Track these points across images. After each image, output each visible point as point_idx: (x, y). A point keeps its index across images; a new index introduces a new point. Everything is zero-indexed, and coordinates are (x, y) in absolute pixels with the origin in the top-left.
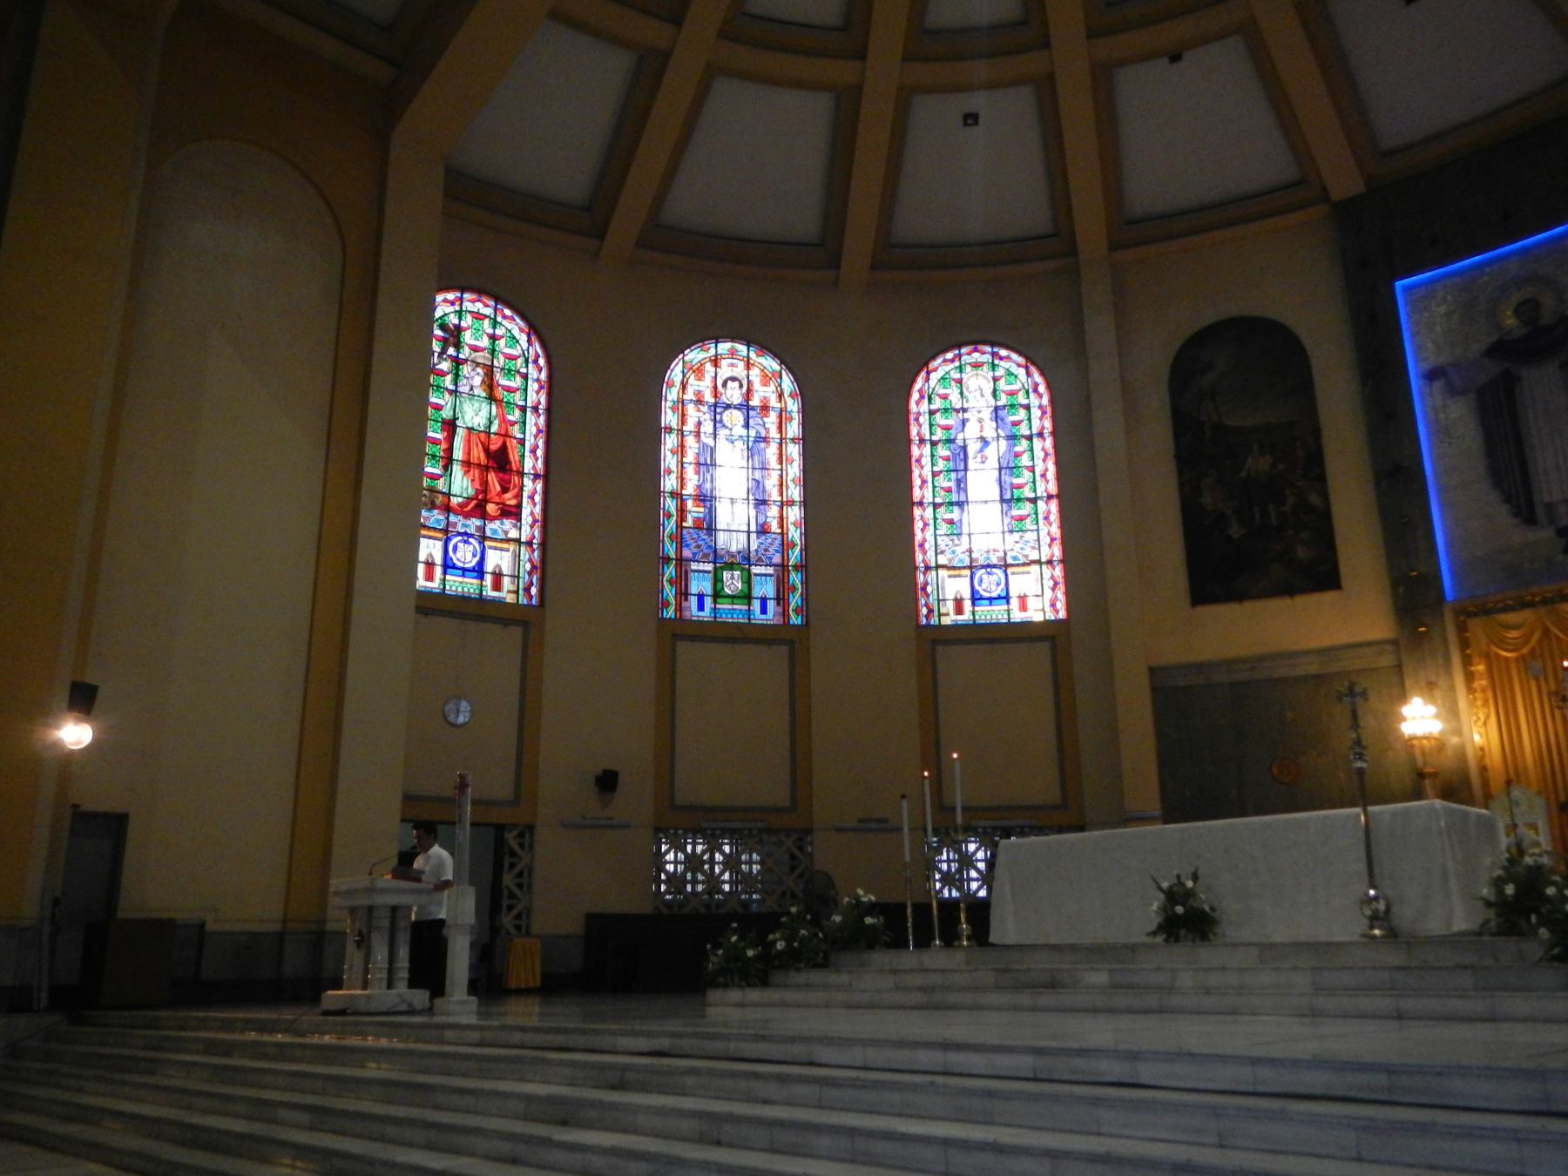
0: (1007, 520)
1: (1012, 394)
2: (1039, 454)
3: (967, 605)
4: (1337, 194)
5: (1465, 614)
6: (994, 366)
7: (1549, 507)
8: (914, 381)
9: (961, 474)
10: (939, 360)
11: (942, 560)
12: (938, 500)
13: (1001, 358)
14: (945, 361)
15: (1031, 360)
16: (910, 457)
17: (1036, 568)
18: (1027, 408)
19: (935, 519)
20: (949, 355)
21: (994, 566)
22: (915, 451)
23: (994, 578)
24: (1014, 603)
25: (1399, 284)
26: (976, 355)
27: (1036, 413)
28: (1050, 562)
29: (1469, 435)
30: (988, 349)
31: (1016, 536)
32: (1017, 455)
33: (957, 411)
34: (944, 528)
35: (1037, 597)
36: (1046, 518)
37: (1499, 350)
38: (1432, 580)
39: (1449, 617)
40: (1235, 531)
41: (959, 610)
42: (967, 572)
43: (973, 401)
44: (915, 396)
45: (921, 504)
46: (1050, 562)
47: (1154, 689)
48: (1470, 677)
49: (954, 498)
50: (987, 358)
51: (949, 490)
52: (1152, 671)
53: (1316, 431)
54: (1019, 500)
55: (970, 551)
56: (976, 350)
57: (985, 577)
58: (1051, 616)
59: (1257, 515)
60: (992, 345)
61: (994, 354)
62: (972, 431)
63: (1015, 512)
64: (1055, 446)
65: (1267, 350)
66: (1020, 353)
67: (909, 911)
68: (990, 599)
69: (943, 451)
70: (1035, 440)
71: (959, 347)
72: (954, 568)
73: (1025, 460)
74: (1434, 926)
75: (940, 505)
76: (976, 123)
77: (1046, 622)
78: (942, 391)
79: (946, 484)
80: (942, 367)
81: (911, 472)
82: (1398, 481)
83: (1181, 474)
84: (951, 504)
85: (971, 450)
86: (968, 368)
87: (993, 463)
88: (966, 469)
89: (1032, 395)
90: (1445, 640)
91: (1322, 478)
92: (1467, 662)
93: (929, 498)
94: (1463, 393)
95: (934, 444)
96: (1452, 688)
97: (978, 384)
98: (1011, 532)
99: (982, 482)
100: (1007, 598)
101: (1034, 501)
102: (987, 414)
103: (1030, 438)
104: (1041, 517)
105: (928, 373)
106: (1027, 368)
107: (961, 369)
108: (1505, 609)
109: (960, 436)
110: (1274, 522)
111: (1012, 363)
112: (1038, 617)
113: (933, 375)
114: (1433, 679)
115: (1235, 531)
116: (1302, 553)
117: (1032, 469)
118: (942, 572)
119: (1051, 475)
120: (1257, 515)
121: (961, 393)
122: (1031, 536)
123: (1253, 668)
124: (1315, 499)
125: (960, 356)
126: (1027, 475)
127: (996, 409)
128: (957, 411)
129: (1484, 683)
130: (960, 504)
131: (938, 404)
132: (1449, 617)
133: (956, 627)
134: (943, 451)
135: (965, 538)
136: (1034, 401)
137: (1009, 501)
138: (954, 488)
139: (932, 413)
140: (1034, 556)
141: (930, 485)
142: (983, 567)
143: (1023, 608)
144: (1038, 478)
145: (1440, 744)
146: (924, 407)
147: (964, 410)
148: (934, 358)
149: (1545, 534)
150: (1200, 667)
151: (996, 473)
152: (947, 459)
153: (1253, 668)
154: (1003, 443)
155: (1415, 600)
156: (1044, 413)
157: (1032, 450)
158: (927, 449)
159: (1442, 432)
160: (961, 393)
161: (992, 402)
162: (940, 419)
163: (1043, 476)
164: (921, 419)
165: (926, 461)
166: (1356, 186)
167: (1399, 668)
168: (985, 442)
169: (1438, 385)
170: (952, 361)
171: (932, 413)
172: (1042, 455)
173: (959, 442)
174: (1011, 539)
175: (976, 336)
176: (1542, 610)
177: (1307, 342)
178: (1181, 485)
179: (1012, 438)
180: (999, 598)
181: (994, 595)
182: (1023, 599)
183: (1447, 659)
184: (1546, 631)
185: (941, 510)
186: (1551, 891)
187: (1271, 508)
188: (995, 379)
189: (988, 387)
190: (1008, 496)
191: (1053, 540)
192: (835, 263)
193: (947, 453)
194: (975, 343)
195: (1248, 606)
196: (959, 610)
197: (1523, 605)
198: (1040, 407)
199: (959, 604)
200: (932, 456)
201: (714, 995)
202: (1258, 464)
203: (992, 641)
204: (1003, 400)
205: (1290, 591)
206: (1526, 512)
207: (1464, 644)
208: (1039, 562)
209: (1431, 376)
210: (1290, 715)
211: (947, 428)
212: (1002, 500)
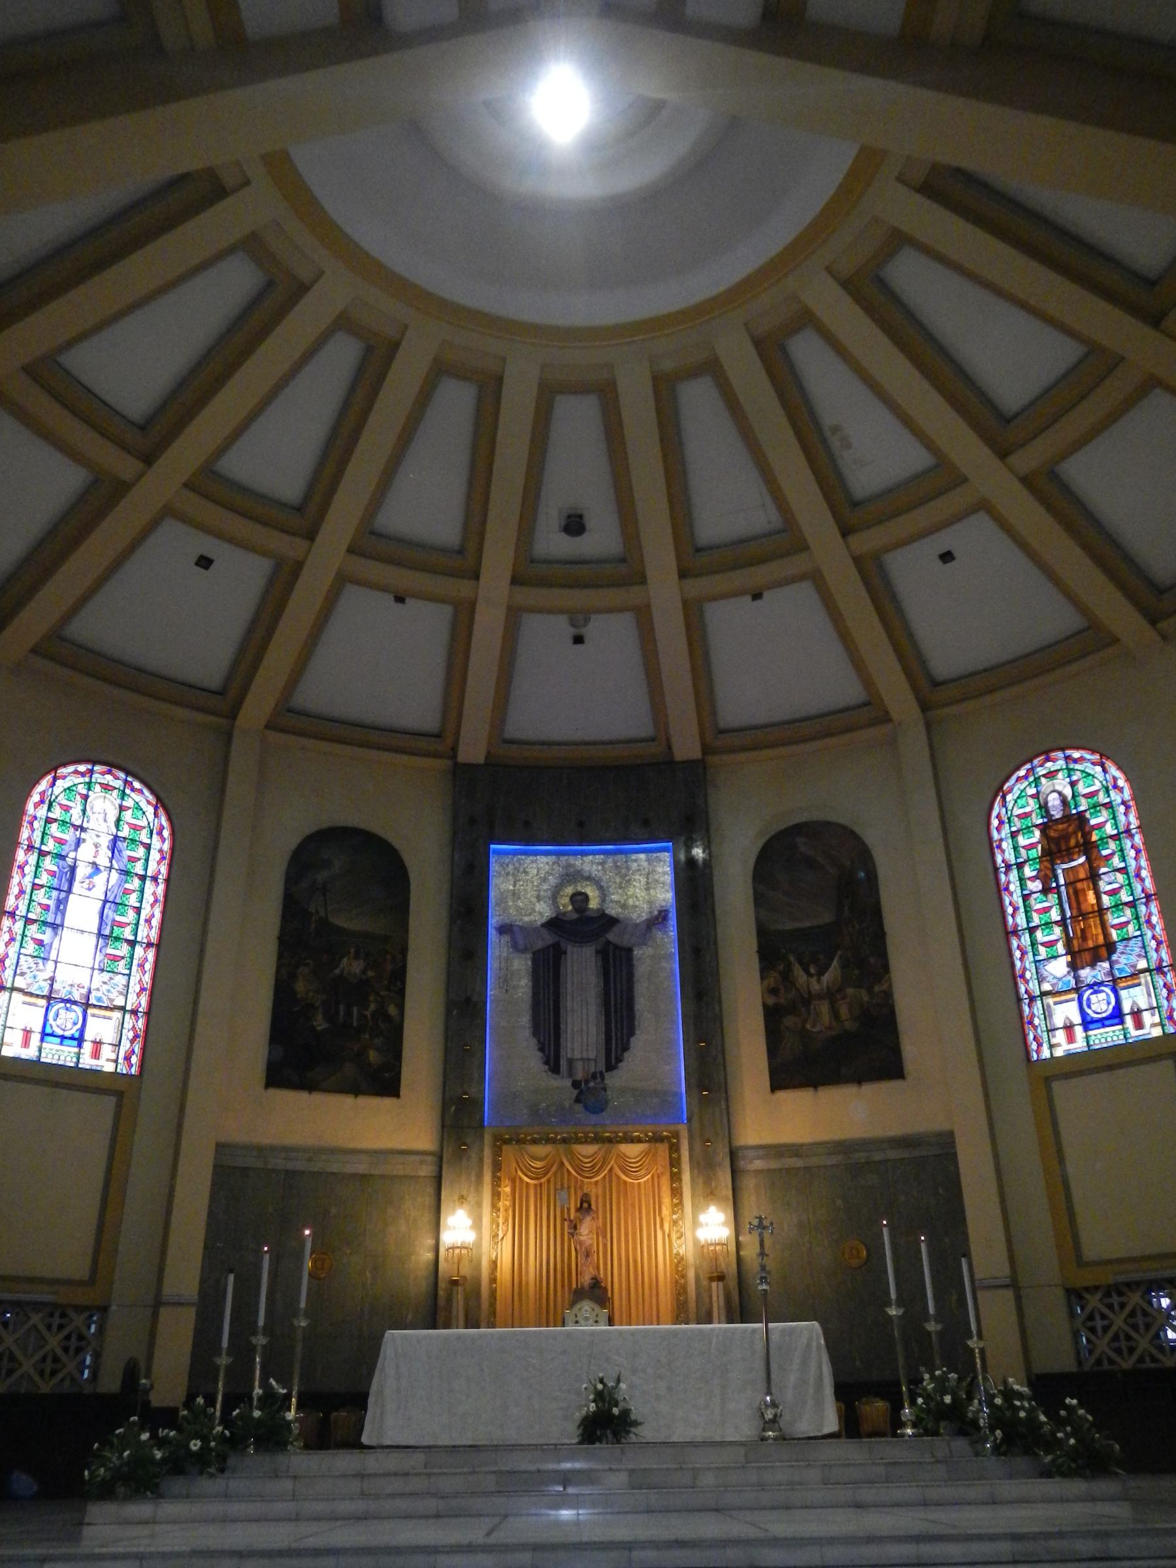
0: (99, 957)
1: (135, 828)
2: (148, 898)
3: (35, 1038)
4: (462, 758)
5: (500, 1141)
6: (123, 795)
7: (570, 1061)
8: (37, 782)
9: (63, 895)
10: (71, 769)
11: (20, 982)
12: (31, 916)
13: (133, 790)
14: (76, 772)
15: (161, 803)
16: (14, 860)
17: (117, 1015)
18: (148, 847)
19: (23, 935)
20: (82, 768)
21: (75, 1003)
22: (20, 856)
23: (73, 1015)
24: (87, 1047)
25: (492, 846)
26: (109, 777)
27: (155, 856)
28: (134, 1012)
29: (523, 986)
30: (122, 775)
31: (106, 976)
32: (127, 892)
33: (76, 827)
34: (30, 947)
35: (109, 1044)
36: (141, 966)
37: (555, 924)
38: (476, 1104)
39: (488, 1139)
40: (320, 1023)
41: (26, 1043)
42: (43, 1002)
43: (92, 823)
44: (35, 797)
45: (12, 915)
46: (134, 1012)
47: (215, 1166)
48: (496, 1195)
49: (50, 918)
50: (118, 784)
51: (46, 908)
52: (220, 1147)
53: (404, 950)
54: (117, 939)
55: (52, 979)
56: (109, 772)
57: (62, 1012)
58: (122, 1068)
59: (342, 1013)
60: (128, 773)
61: (126, 782)
62: (85, 853)
63: (110, 951)
64: (166, 896)
65: (374, 864)
66: (153, 792)
68: (63, 1038)
69: (49, 864)
70: (148, 882)
71: (94, 763)
72: (31, 994)
73: (133, 900)
74: (804, 1427)
75: (34, 921)
76: (207, 568)
77: (115, 1073)
78: (65, 802)
79: (46, 902)
80: (70, 777)
81: (10, 877)
82: (464, 1011)
83: (280, 957)
84: (45, 923)
85: (82, 871)
86: (98, 788)
87: (99, 892)
88: (69, 891)
89: (155, 836)
90: (481, 1160)
91: (401, 993)
92: (496, 1182)
93: (22, 910)
94: (525, 950)
95: (42, 854)
96: (479, 1205)
97: (103, 806)
98: (102, 970)
100: (80, 1040)
101: (132, 944)
102: (105, 841)
103: (143, 878)
104: (135, 962)
105: (55, 779)
106: (156, 808)
107: (89, 785)
108: (535, 1142)
109: (72, 855)
110: (355, 1024)
111: (143, 799)
112: (109, 1068)
113: (59, 782)
114: (465, 1193)
115: (320, 1023)
116: (373, 1056)
117: (138, 910)
118: (15, 994)
119: (155, 922)
120: (342, 1013)
121: (84, 811)
122: (121, 980)
123: (310, 1160)
124: (392, 1010)
125: (91, 772)
126: (131, 916)
127: (116, 838)
128: (76, 827)
129: (508, 1203)
130: (56, 927)
131: (57, 813)
132: (488, 1139)
133: (16, 1060)
134: (49, 864)
135: (50, 965)
136: (156, 843)
137: (106, 937)
138: (52, 908)
139: (49, 821)
140: (120, 1001)
141: (27, 896)
142: (63, 1001)
143: (96, 1054)
144: (142, 922)
146: (42, 812)
147: (83, 829)
148: (65, 765)
150: (261, 1150)
151: (100, 903)
152: (53, 874)
153: (310, 1160)
154: (115, 876)
155: (460, 1120)
156: (163, 858)
157: (142, 891)
158: (33, 858)
159: (506, 981)
160: (84, 811)
161: (114, 831)
162: (54, 829)
163: (148, 921)
164: (36, 824)
165: (27, 869)
166: (481, 759)
167: (438, 1181)
168: (96, 868)
169: (506, 938)
170: (83, 774)
171: (49, 821)
172: (152, 899)
173: (69, 861)
174: (99, 978)
175: (130, 767)
176: (561, 1147)
178: (279, 967)
179: (125, 873)
180: (72, 1038)
181: (68, 1034)
182: (98, 1044)
183: (480, 1176)
184: (562, 1164)
185: (33, 930)
186: (948, 1399)
187: (355, 1009)
188: (122, 808)
189: (113, 815)
190: (107, 932)
191: (143, 989)
193: (55, 868)
194: (112, 766)
195: (317, 1098)
196: (26, 1043)
197: (548, 1141)
198: (161, 851)
199: (27, 1033)
200: (38, 866)
201: (97, 1511)
202: (351, 966)
203: (56, 1085)
204: (125, 832)
205: (356, 1090)
207: (497, 1167)
208: (123, 1009)
210: (334, 1211)
211: (61, 842)
212: (100, 934)
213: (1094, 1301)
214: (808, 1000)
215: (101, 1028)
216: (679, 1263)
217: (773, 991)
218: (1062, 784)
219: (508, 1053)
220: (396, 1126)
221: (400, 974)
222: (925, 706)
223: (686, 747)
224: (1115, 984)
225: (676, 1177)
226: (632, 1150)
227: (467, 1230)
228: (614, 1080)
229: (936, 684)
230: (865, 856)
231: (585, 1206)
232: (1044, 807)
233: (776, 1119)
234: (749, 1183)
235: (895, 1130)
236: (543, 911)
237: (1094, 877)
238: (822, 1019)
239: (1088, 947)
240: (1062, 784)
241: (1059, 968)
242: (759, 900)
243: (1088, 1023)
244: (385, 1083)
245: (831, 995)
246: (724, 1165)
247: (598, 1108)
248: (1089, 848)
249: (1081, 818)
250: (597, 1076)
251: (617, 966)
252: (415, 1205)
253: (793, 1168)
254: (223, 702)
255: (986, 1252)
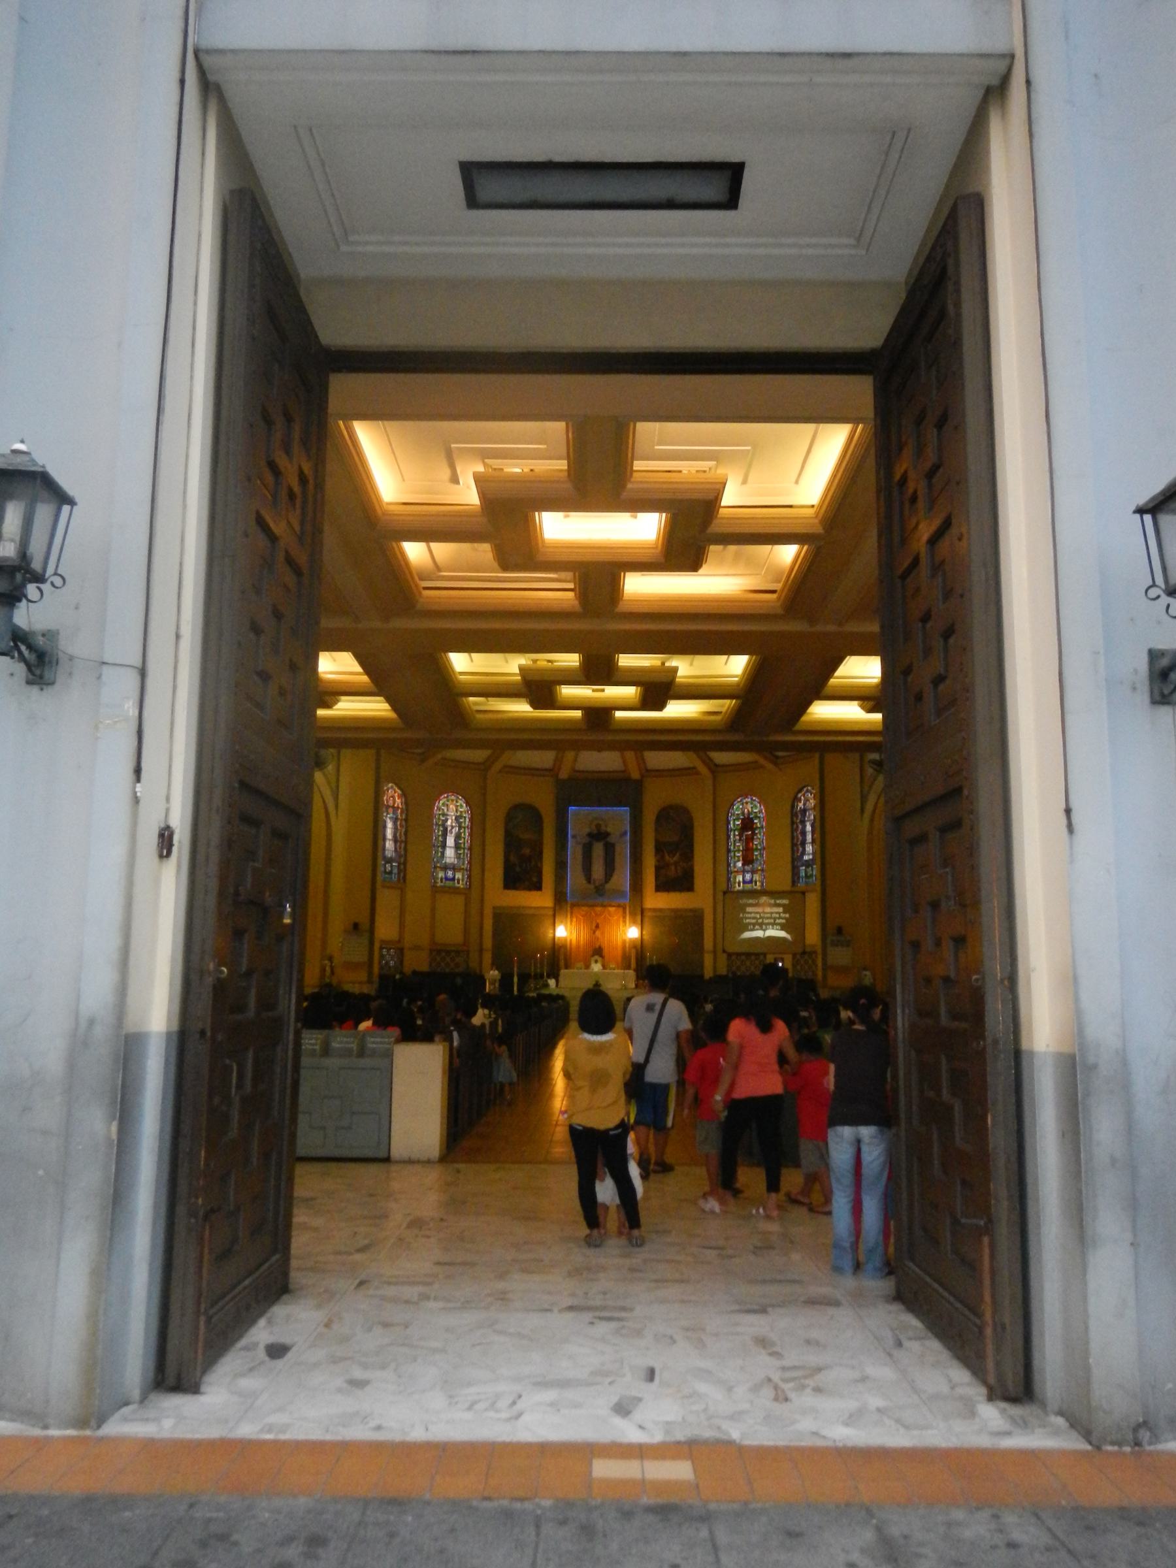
5: (573, 905)
15: (467, 803)
25: (572, 809)
29: (580, 857)
37: (590, 835)
53: (541, 844)
62: (449, 823)
65: (532, 815)
67: (516, 979)
82: (561, 866)
99: (450, 841)
100: (453, 879)
111: (461, 802)
115: (518, 869)
116: (535, 879)
145: (566, 939)
149: (592, 887)
155: (560, 899)
177: (544, 816)
179: (460, 827)
192: (423, 761)
202: (527, 851)
205: (530, 889)
206: (589, 879)
209: (574, 837)
213: (734, 957)
214: (668, 865)
215: (458, 875)
216: (624, 942)
217: (658, 861)
218: (749, 806)
219: (574, 877)
220: (542, 900)
221: (541, 853)
222: (713, 772)
223: (635, 775)
224: (753, 872)
225: (624, 917)
226: (612, 909)
227: (562, 932)
228: (608, 886)
229: (716, 765)
230: (691, 819)
231: (597, 926)
232: (743, 813)
233: (655, 900)
234: (646, 919)
235: (691, 906)
236: (587, 830)
237: (752, 839)
238: (672, 872)
239: (748, 860)
240: (749, 806)
241: (740, 864)
242: (656, 830)
243: (744, 882)
244: (538, 887)
245: (676, 864)
246: (640, 914)
247: (601, 895)
248: (753, 830)
249: (751, 820)
250: (602, 885)
251: (610, 850)
252: (548, 922)
253: (660, 916)
254: (484, 768)
255: (708, 943)
